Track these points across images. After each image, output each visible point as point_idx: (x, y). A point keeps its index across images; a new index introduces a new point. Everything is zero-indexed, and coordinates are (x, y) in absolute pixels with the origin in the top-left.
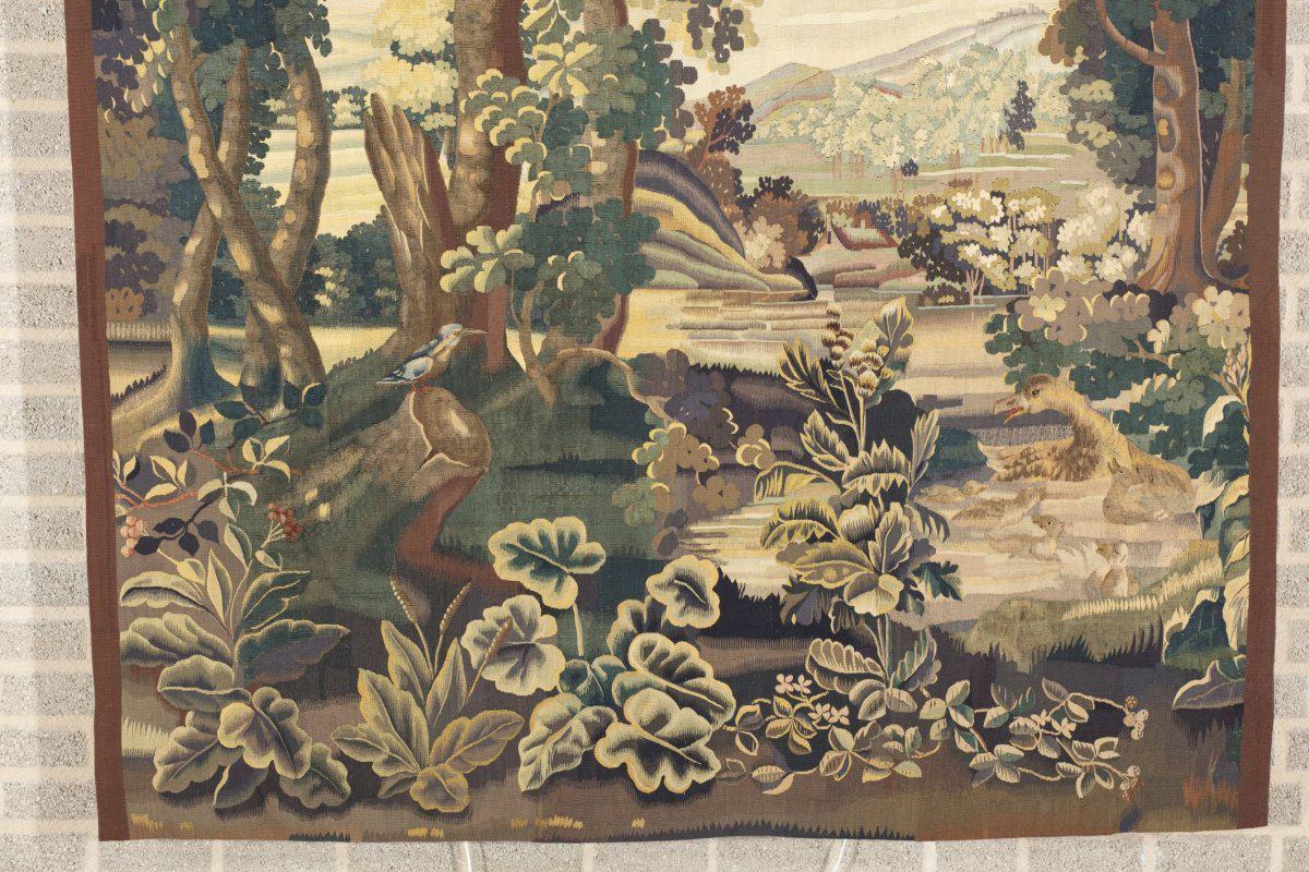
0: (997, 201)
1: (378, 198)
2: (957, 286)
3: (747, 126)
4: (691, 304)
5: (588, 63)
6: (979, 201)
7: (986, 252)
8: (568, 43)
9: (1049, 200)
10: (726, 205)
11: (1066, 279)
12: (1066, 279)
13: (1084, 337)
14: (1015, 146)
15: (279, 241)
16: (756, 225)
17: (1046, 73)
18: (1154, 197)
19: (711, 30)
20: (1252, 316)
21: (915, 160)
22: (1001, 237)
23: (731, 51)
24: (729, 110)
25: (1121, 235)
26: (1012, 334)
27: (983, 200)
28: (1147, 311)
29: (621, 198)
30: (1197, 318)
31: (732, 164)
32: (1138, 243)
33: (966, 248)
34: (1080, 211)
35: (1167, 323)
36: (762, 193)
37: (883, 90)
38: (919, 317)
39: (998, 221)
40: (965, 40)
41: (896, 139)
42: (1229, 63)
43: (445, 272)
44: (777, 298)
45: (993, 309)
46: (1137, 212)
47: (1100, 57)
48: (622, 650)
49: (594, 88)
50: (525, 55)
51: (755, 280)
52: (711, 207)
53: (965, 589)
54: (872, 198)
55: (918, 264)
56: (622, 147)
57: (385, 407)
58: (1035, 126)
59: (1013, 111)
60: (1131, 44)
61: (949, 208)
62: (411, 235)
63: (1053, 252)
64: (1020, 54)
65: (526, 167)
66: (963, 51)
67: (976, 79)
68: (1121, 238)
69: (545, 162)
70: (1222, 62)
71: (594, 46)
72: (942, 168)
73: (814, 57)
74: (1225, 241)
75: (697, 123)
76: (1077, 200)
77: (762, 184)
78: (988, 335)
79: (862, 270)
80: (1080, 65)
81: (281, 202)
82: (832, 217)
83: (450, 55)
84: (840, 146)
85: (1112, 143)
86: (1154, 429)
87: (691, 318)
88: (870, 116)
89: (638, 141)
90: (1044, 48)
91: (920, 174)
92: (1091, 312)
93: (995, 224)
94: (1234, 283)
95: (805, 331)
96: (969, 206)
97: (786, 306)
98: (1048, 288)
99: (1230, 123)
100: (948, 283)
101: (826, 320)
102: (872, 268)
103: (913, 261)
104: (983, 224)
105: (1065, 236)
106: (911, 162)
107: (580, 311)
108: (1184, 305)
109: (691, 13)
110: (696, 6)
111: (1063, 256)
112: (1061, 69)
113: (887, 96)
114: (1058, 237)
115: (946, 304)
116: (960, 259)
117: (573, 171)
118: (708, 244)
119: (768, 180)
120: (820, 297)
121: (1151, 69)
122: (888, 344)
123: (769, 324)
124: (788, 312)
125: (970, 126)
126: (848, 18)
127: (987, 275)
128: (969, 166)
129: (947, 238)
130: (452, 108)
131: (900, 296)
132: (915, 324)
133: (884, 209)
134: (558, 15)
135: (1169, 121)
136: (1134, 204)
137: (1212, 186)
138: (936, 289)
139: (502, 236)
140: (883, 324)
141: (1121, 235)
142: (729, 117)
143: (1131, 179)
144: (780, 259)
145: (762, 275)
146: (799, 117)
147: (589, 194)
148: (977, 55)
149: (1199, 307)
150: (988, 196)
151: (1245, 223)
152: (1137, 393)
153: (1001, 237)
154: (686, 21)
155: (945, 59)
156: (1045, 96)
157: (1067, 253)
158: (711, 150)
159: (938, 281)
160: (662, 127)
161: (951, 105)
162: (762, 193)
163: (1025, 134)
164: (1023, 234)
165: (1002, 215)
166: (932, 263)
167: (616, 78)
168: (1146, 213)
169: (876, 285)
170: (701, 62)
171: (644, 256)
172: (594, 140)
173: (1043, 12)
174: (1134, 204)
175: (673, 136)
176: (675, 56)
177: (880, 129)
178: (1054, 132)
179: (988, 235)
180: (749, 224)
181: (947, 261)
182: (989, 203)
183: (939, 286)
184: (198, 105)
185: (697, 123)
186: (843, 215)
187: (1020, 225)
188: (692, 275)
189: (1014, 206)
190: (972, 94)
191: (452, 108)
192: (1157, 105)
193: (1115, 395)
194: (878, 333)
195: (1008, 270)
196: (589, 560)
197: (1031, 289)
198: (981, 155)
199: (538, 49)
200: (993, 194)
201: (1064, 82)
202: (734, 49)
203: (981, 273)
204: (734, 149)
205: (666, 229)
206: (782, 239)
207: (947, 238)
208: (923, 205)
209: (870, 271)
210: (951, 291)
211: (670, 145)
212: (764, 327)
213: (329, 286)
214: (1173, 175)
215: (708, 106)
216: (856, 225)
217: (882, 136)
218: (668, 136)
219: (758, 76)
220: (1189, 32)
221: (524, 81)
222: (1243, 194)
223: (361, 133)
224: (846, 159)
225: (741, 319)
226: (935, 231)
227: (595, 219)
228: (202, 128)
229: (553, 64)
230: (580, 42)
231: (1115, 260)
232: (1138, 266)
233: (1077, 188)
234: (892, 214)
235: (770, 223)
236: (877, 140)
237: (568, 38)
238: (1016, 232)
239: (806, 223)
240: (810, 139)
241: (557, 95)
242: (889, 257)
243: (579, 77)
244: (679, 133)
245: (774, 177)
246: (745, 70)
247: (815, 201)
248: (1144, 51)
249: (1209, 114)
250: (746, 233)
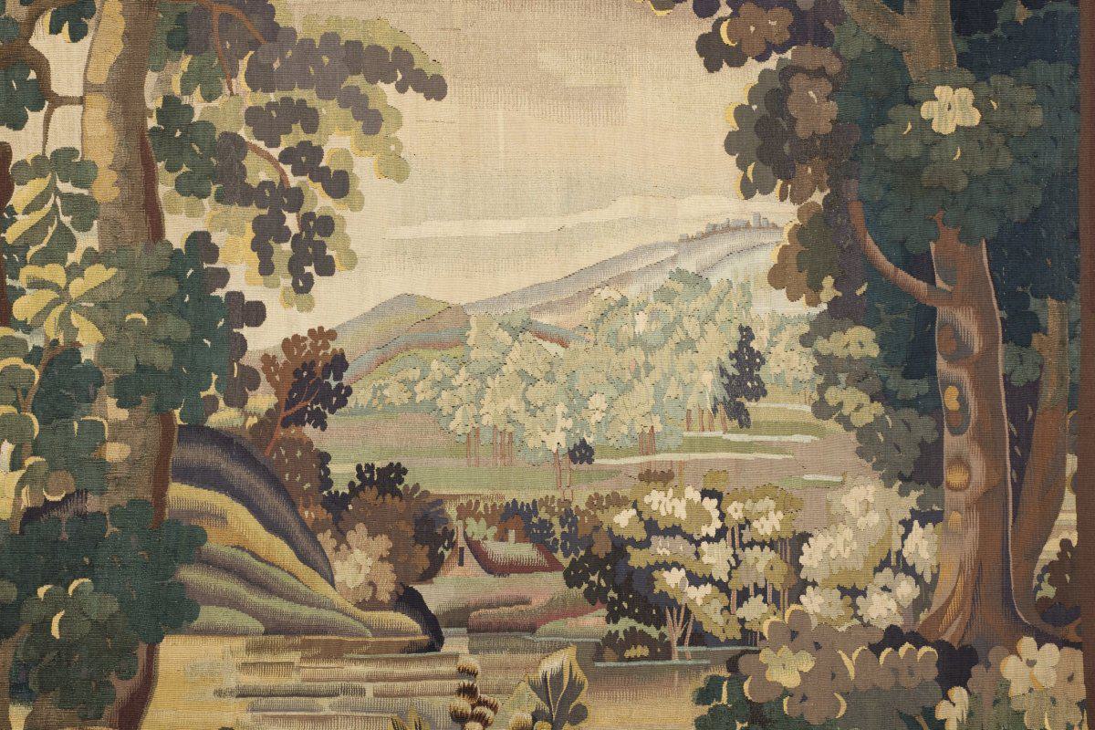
0: (710, 504)
2: (653, 632)
3: (340, 387)
4: (252, 658)
5: (104, 295)
6: (684, 502)
7: (695, 580)
8: (74, 264)
9: (787, 504)
10: (306, 507)
11: (815, 622)
12: (815, 622)
13: (842, 712)
14: (736, 422)
16: (351, 536)
17: (780, 315)
18: (941, 502)
19: (287, 247)
20: (1088, 681)
21: (589, 441)
22: (716, 558)
23: (316, 278)
24: (313, 363)
25: (893, 557)
26: (735, 706)
27: (690, 502)
28: (933, 672)
29: (149, 497)
30: (1007, 684)
31: (316, 445)
32: (919, 570)
33: (666, 574)
34: (832, 520)
35: (964, 692)
36: (362, 487)
37: (542, 335)
38: (600, 679)
39: (713, 534)
40: (659, 264)
41: (561, 408)
42: (1045, 305)
44: (385, 647)
45: (707, 668)
46: (916, 523)
47: (859, 292)
49: (112, 333)
50: (9, 282)
51: (351, 621)
52: (283, 509)
54: (525, 498)
55: (594, 596)
56: (153, 421)
58: (765, 393)
59: (732, 371)
60: (902, 275)
61: (639, 513)
63: (794, 582)
64: (742, 286)
66: (659, 279)
67: (678, 321)
68: (893, 562)
69: (36, 443)
70: (1034, 304)
71: (113, 271)
72: (629, 453)
73: (441, 285)
74: (1045, 569)
75: (264, 384)
76: (829, 504)
77: (361, 475)
78: (700, 707)
79: (511, 605)
80: (829, 304)
82: (465, 526)
84: (477, 418)
85: (878, 419)
87: (253, 680)
88: (522, 374)
89: (177, 412)
90: (777, 277)
91: (597, 461)
92: (852, 674)
93: (708, 539)
94: (1060, 632)
95: (426, 699)
96: (670, 511)
97: (396, 660)
98: (789, 635)
99: (1048, 394)
100: (640, 627)
101: (455, 682)
102: (526, 602)
103: (587, 594)
104: (690, 538)
105: (811, 557)
106: (583, 442)
107: (85, 671)
108: (988, 665)
109: (258, 223)
110: (265, 212)
111: (809, 589)
112: (801, 310)
113: (546, 344)
114: (802, 560)
115: (636, 659)
116: (656, 591)
117: (78, 458)
118: (278, 567)
119: (370, 468)
120: (447, 648)
121: (934, 310)
122: (549, 719)
123: (370, 688)
124: (399, 670)
125: (669, 392)
126: (489, 228)
127: (696, 615)
128: (668, 451)
129: (638, 559)
131: (565, 646)
132: (589, 691)
133: (543, 514)
134: (60, 222)
135: (960, 388)
136: (912, 511)
137: (1025, 487)
138: (621, 635)
140: (542, 688)
141: (893, 557)
142: (311, 374)
143: (907, 473)
144: (386, 590)
145: (359, 612)
146: (417, 373)
147: (102, 492)
148: (679, 287)
149: (1011, 667)
150: (697, 496)
151: (1074, 543)
153: (716, 558)
154: (250, 235)
155: (632, 291)
156: (780, 349)
157: (814, 584)
158: (285, 424)
159: (625, 624)
160: (212, 391)
161: (641, 359)
162: (362, 487)
163: (750, 405)
164: (750, 554)
165: (718, 524)
166: (616, 596)
167: (145, 319)
168: (930, 526)
169: (532, 629)
170: (271, 294)
171: (182, 585)
172: (113, 412)
173: (775, 227)
174: (912, 511)
175: (229, 403)
176: (232, 286)
177: (537, 394)
178: (793, 401)
179: (697, 554)
180: (340, 535)
181: (636, 593)
182: (700, 508)
183: (625, 632)
185: (264, 384)
186: (483, 521)
187: (745, 540)
188: (254, 613)
189: (735, 511)
190: (671, 344)
192: (941, 364)
194: (535, 702)
195: (727, 608)
197: (763, 637)
198: (686, 434)
199: (27, 272)
200: (705, 493)
201: (806, 329)
202: (320, 273)
203: (688, 612)
204: (320, 422)
205: (216, 543)
206: (391, 557)
207: (638, 559)
208: (602, 508)
209: (522, 607)
210: (644, 639)
211: (224, 417)
212: (362, 692)
214: (968, 470)
215: (282, 358)
216: (502, 537)
217: (540, 404)
218: (222, 403)
219: (357, 313)
220: (985, 260)
222: (1070, 499)
224: (486, 437)
225: (328, 680)
226: (620, 547)
227: (111, 529)
229: (50, 295)
230: (93, 263)
231: (885, 595)
232: (920, 604)
233: (828, 486)
234: (555, 521)
235: (373, 533)
236: (533, 410)
237: (73, 258)
238: (739, 551)
239: (425, 534)
240: (432, 406)
241: (56, 342)
242: (549, 586)
243: (89, 315)
244: (237, 401)
245: (378, 465)
246: (337, 304)
247: (440, 501)
248: (922, 286)
249: (1018, 381)
250: (337, 549)
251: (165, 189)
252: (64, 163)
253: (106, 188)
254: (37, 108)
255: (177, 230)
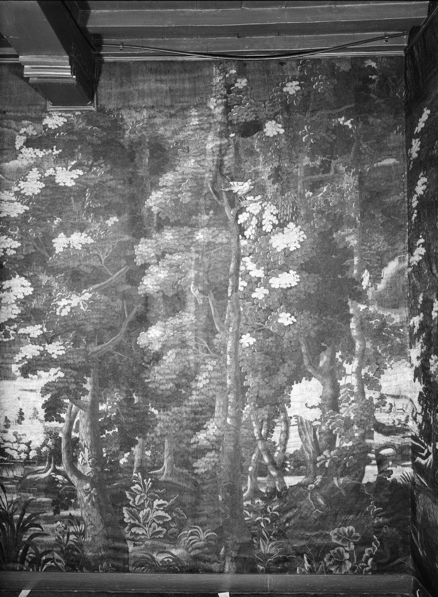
1: (301, 443)
5: (355, 408)
15: (276, 454)
43: (318, 462)
48: (366, 562)
57: (302, 497)
62: (309, 453)
65: (338, 434)
81: (276, 445)
83: (320, 406)
130: (320, 420)
139: (332, 453)
184: (257, 420)
191: (320, 420)
196: (356, 537)
213: (289, 466)
221: (339, 413)
223: (297, 427)
228: (258, 427)
251: (366, 389)
252: (349, 385)
253: (356, 390)
254: (344, 376)
255: (367, 397)
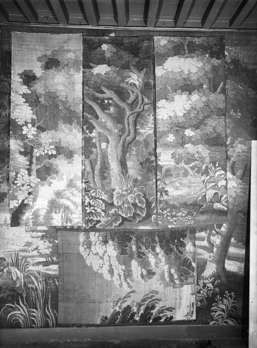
53: (169, 195)
86: (196, 169)
152: (193, 164)
193: (190, 164)
